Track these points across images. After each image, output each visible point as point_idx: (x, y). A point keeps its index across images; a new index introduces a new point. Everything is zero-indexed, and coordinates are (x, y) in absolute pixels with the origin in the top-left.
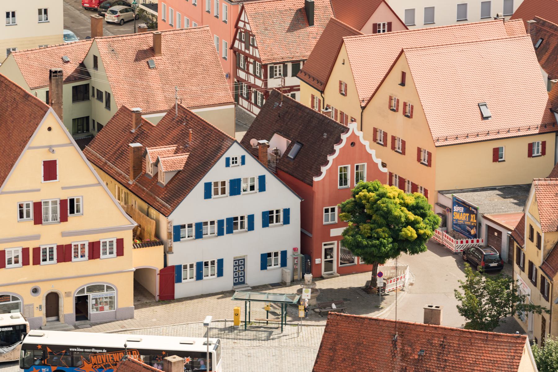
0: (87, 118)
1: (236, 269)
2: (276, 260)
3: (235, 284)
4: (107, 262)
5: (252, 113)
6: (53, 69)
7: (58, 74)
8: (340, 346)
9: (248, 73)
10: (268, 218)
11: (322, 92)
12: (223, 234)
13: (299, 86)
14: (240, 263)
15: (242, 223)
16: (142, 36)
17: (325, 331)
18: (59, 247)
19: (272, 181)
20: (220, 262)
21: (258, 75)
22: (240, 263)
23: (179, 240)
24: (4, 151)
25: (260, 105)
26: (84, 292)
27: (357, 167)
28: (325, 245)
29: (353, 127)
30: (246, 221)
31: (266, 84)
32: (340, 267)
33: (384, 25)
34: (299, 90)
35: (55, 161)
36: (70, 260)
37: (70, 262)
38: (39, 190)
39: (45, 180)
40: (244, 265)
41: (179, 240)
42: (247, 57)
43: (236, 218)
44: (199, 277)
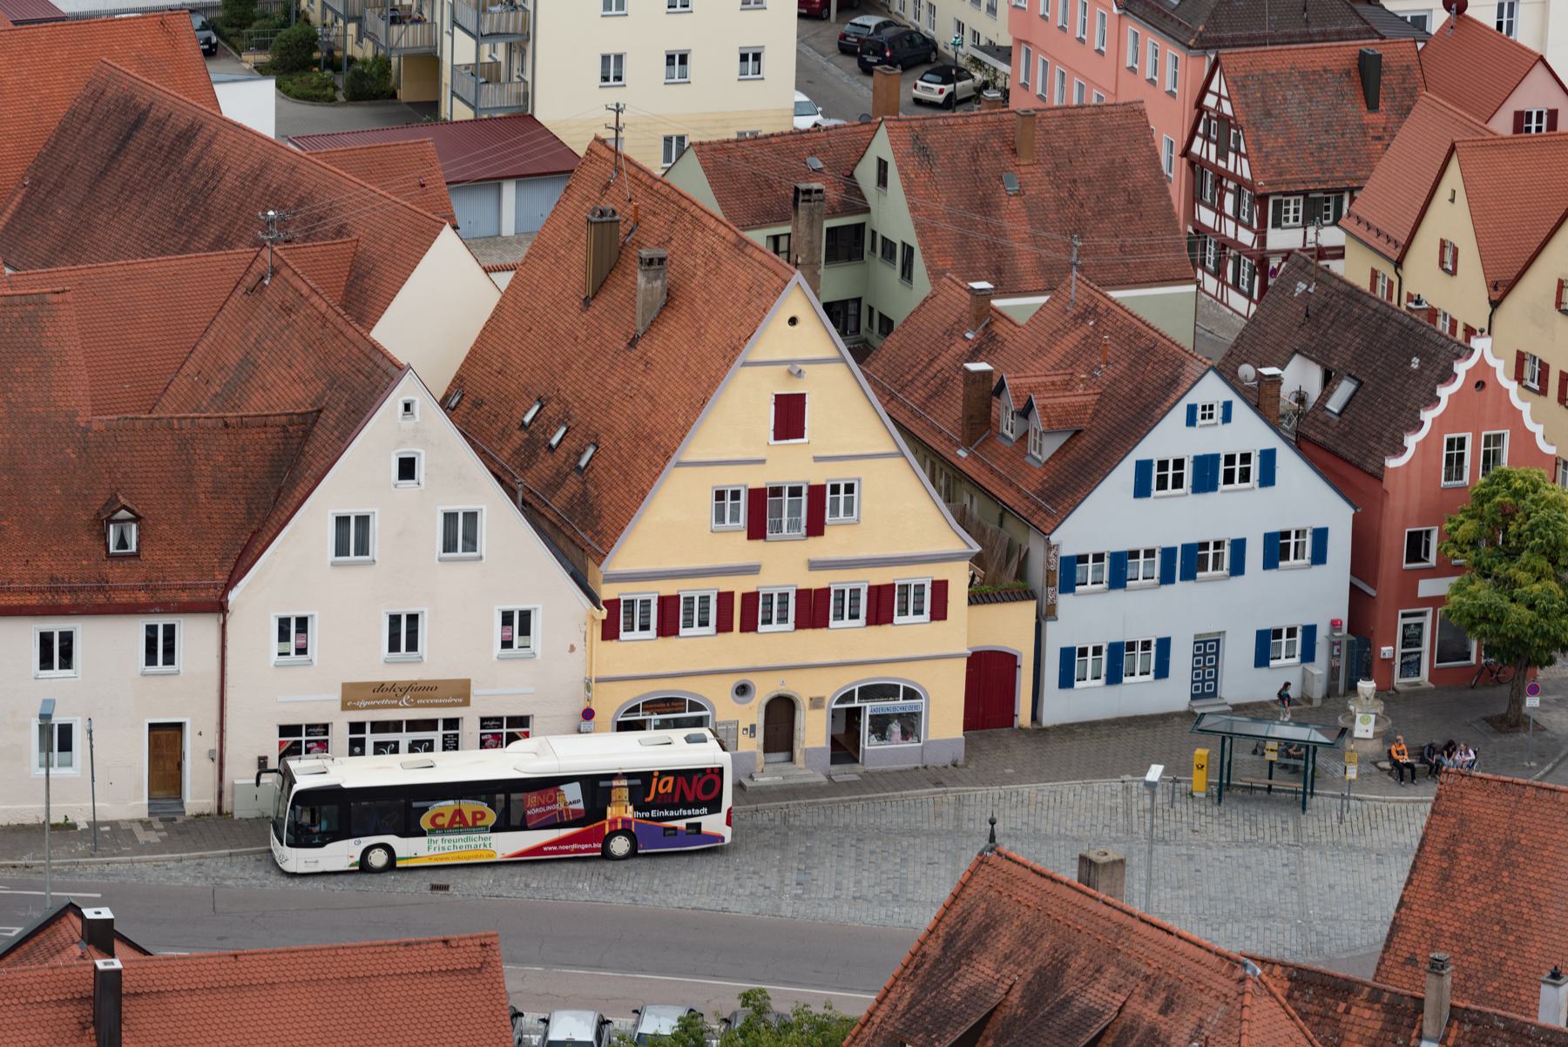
0: (858, 300)
1: (1198, 662)
2: (1291, 646)
3: (1193, 697)
4: (911, 631)
5: (1227, 305)
6: (803, 186)
7: (815, 196)
8: (1465, 845)
9: (1220, 212)
10: (1277, 548)
11: (1399, 264)
12: (1172, 581)
13: (1343, 248)
14: (1208, 649)
15: (1216, 556)
16: (990, 118)
17: (1433, 811)
18: (802, 595)
19: (1290, 464)
20: (1164, 645)
21: (1245, 218)
22: (1208, 649)
23: (1124, 586)
24: (686, 367)
25: (1245, 288)
26: (852, 700)
27: (1487, 438)
28: (1404, 616)
29: (1478, 344)
30: (1227, 551)
31: (1262, 241)
32: (1438, 669)
33: (1540, 114)
34: (1342, 256)
35: (802, 396)
36: (825, 624)
37: (824, 630)
38: (763, 461)
39: (776, 438)
40: (1217, 654)
41: (1124, 586)
42: (1220, 176)
43: (1205, 546)
44: (1114, 677)
